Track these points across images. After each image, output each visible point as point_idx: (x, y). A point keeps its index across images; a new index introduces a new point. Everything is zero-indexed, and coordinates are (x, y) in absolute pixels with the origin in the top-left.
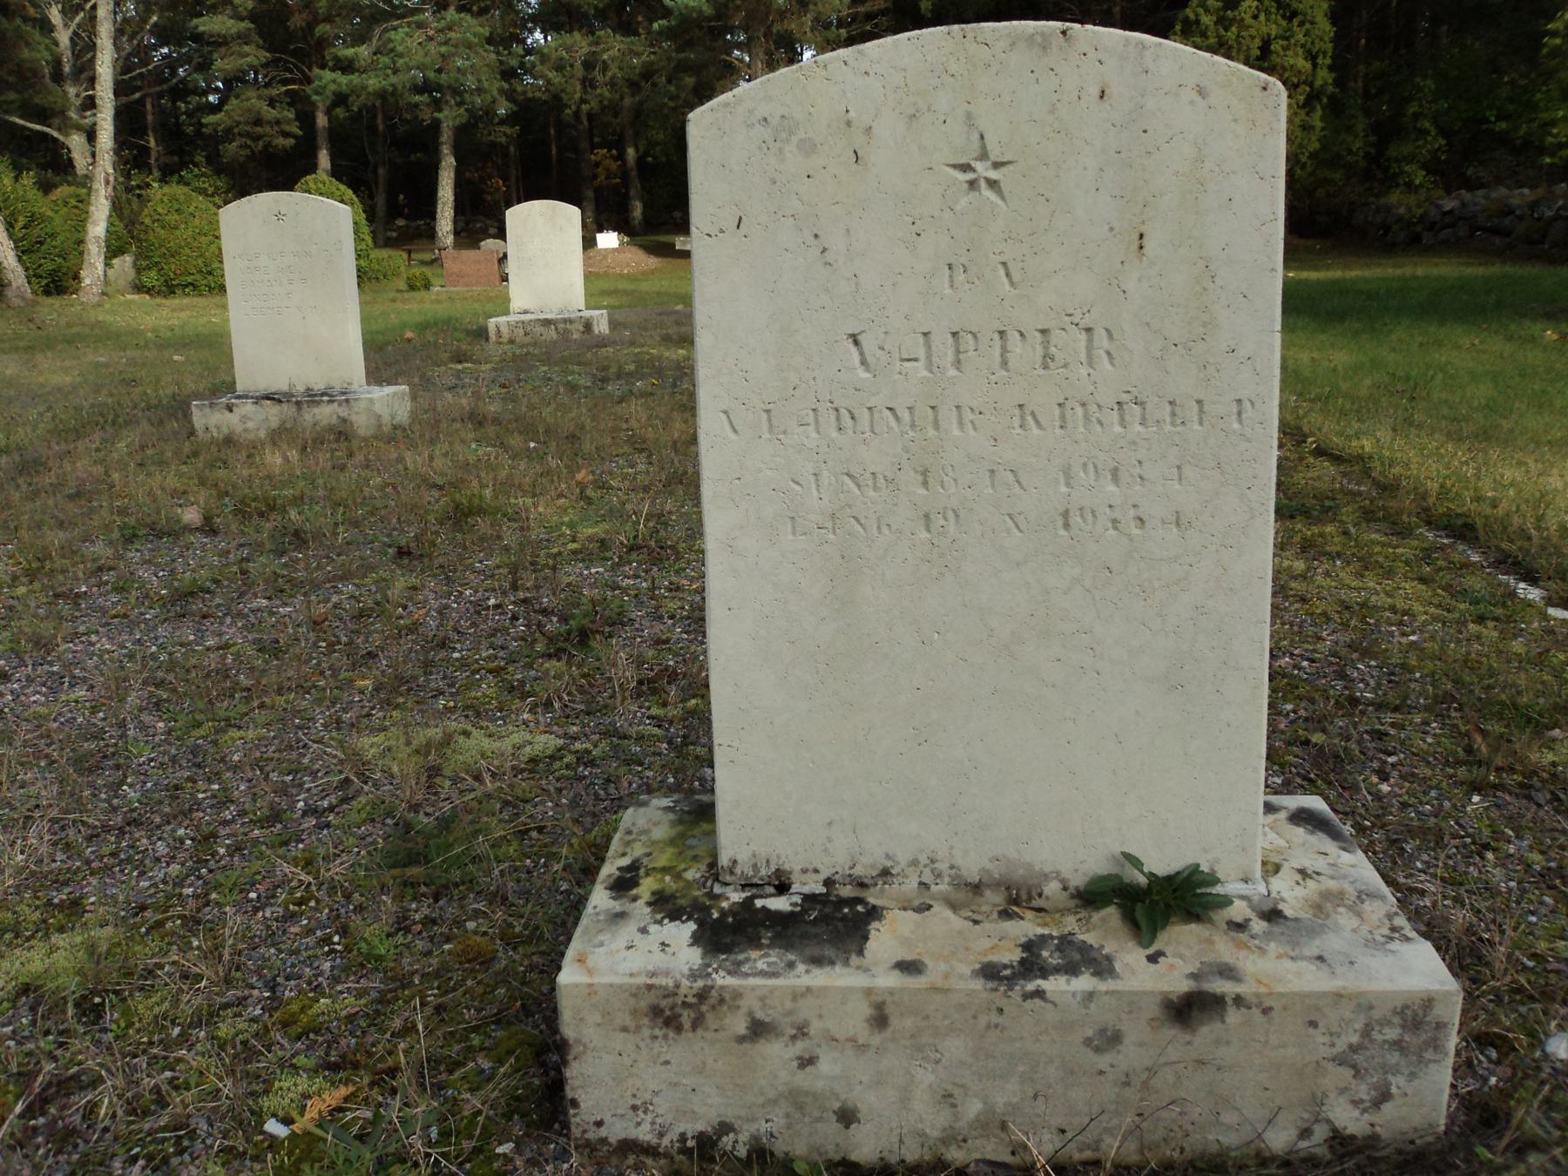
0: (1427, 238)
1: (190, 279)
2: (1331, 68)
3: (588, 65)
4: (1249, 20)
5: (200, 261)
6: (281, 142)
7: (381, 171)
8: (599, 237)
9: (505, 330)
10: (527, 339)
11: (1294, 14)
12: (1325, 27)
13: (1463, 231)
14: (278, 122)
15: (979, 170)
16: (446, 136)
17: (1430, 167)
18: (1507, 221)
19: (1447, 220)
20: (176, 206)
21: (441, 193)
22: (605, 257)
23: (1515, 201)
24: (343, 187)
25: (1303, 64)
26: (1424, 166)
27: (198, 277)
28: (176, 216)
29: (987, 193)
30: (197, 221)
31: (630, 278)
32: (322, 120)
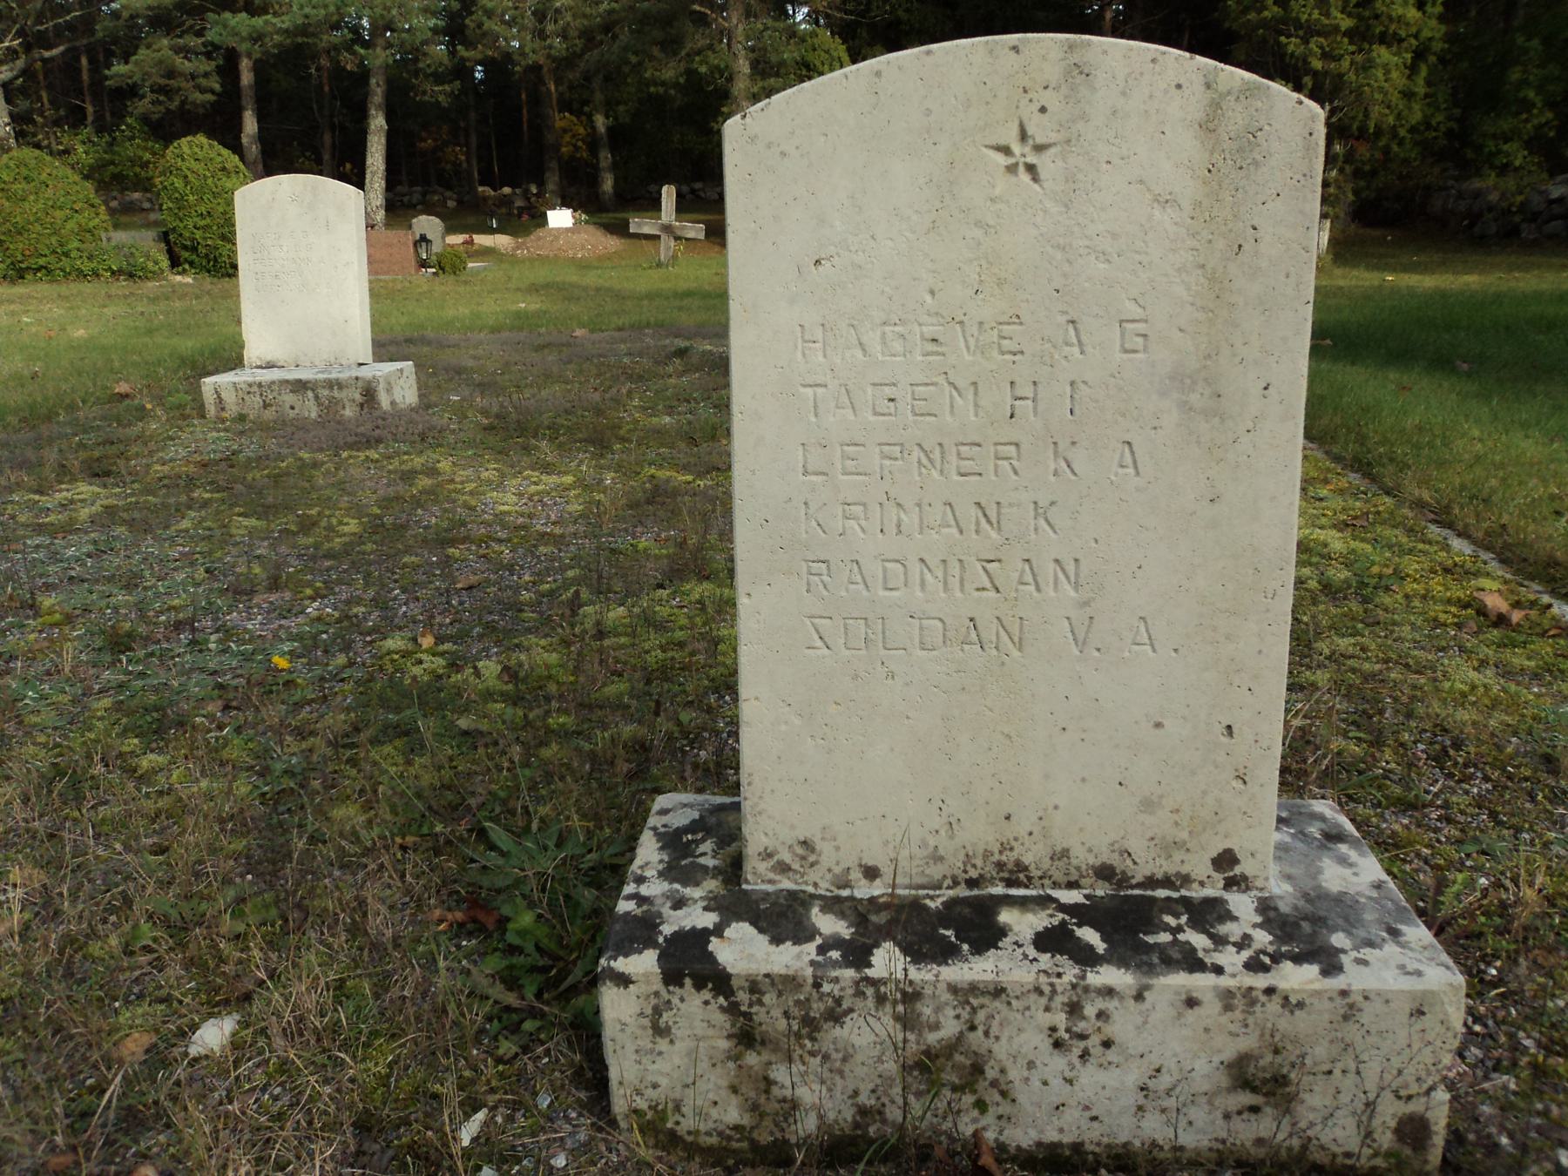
0: (1528, 231)
1: (42, 261)
2: (1441, 18)
5: (54, 240)
6: (198, 97)
7: (327, 138)
8: (550, 214)
9: (229, 397)
10: (269, 414)
14: (193, 77)
16: (377, 91)
17: (1534, 144)
19: (1556, 209)
20: (25, 172)
21: (369, 161)
22: (557, 238)
24: (225, 152)
26: (1529, 144)
27: (52, 259)
28: (24, 185)
29: (1025, 177)
30: (50, 191)
31: (583, 266)
32: (247, 78)
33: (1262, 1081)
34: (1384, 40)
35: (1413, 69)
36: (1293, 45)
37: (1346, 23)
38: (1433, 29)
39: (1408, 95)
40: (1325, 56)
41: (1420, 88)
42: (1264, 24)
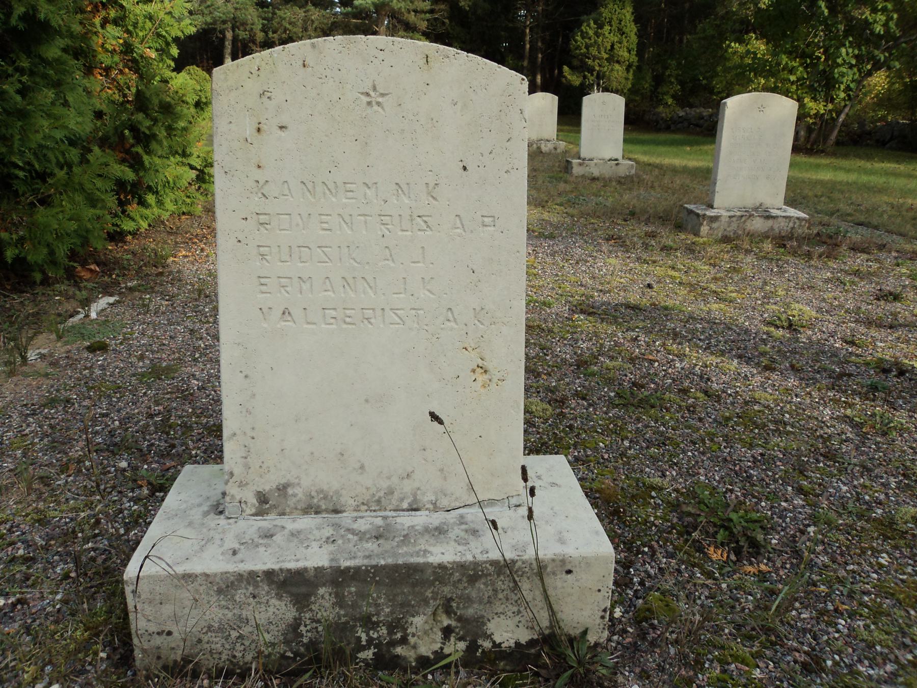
0: (673, 127)
3: (305, 21)
4: (607, 35)
11: (624, 33)
12: (634, 39)
13: (686, 124)
15: (604, 103)
17: (674, 97)
18: (702, 121)
23: (705, 114)
25: (626, 54)
26: (673, 97)
33: (555, 149)
34: (618, 62)
35: (628, 70)
36: (590, 62)
37: (606, 56)
38: (634, 59)
39: (627, 79)
40: (600, 66)
41: (631, 76)
42: (581, 54)
